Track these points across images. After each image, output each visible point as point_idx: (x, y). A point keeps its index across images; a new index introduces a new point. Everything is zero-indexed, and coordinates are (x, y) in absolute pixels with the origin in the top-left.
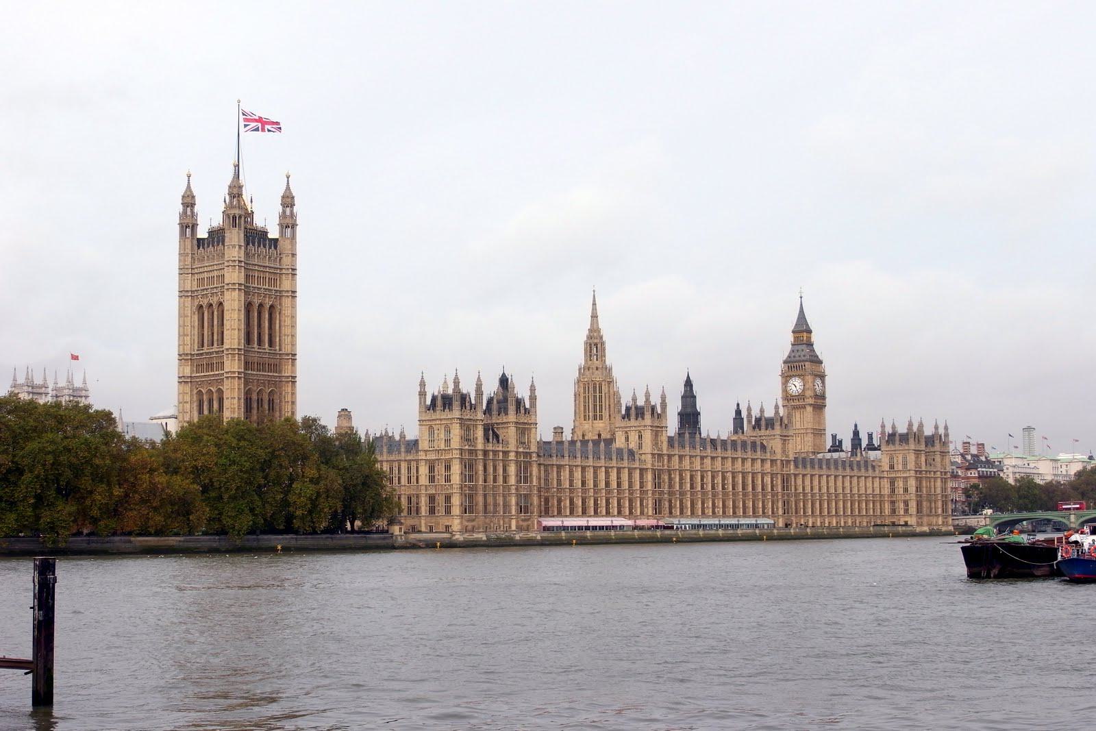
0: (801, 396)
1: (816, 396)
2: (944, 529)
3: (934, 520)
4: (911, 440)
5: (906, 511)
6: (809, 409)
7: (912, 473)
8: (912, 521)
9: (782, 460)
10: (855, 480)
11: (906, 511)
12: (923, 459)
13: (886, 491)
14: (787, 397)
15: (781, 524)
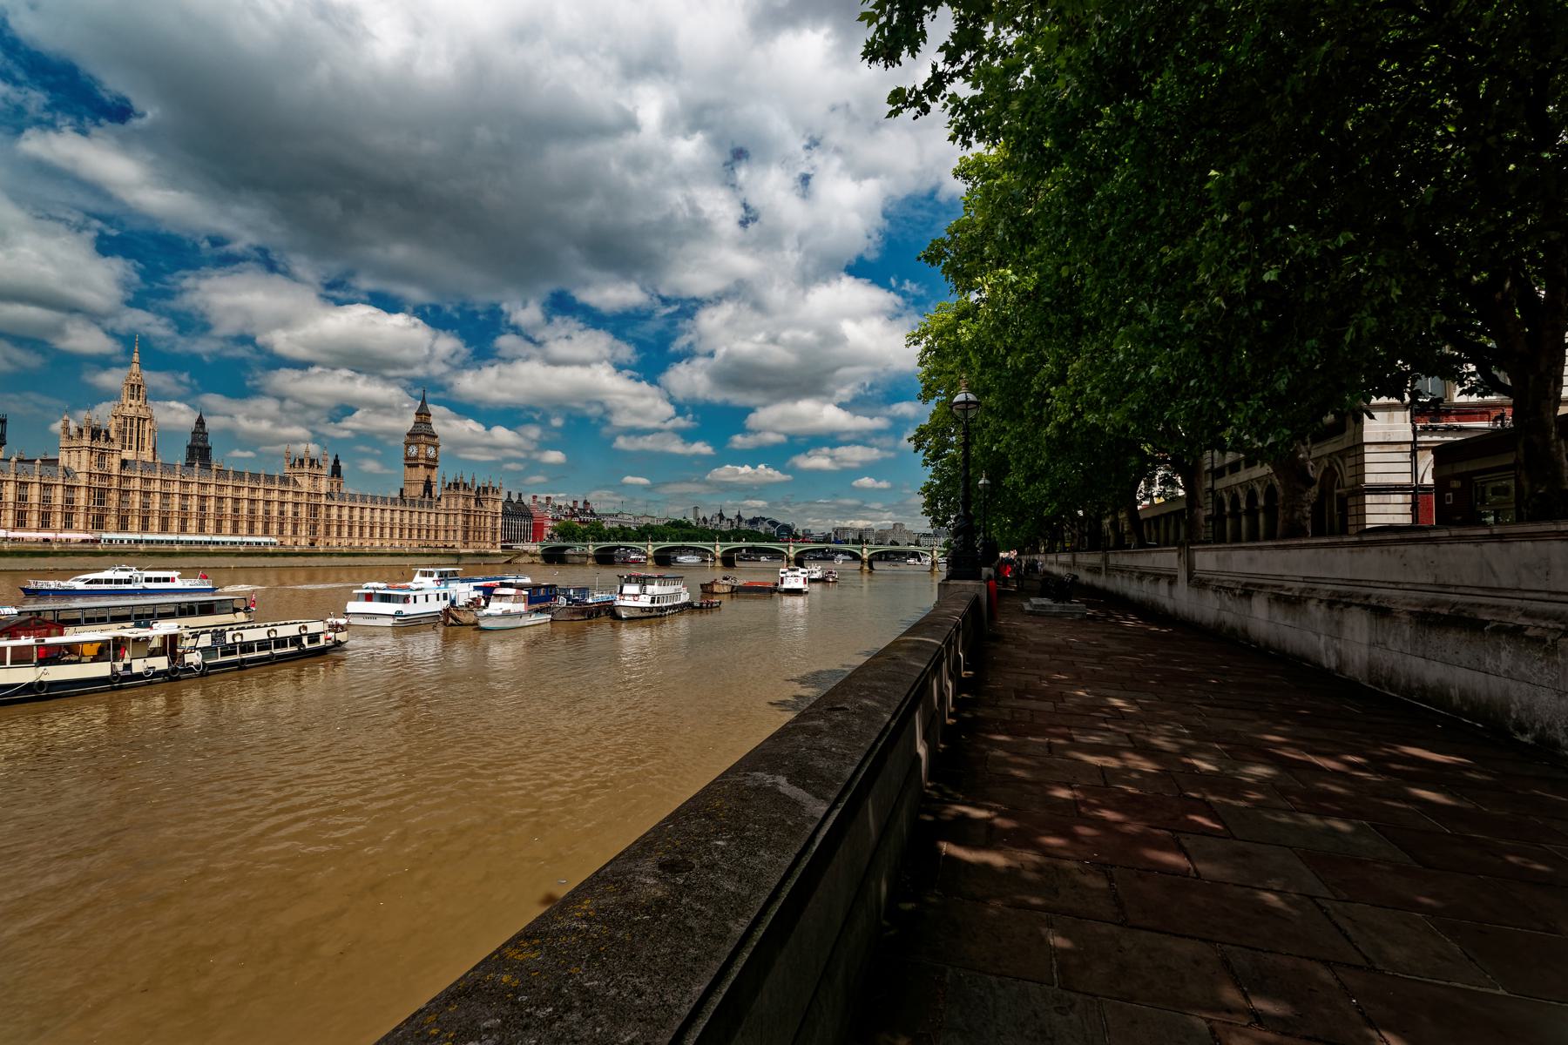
0: (416, 458)
1: (427, 459)
2: (491, 551)
3: (482, 545)
4: (461, 488)
5: (455, 537)
6: (422, 467)
7: (460, 512)
8: (458, 545)
9: (309, 494)
10: (407, 515)
11: (455, 537)
12: (473, 502)
13: (442, 522)
14: (407, 458)
15: (304, 542)
